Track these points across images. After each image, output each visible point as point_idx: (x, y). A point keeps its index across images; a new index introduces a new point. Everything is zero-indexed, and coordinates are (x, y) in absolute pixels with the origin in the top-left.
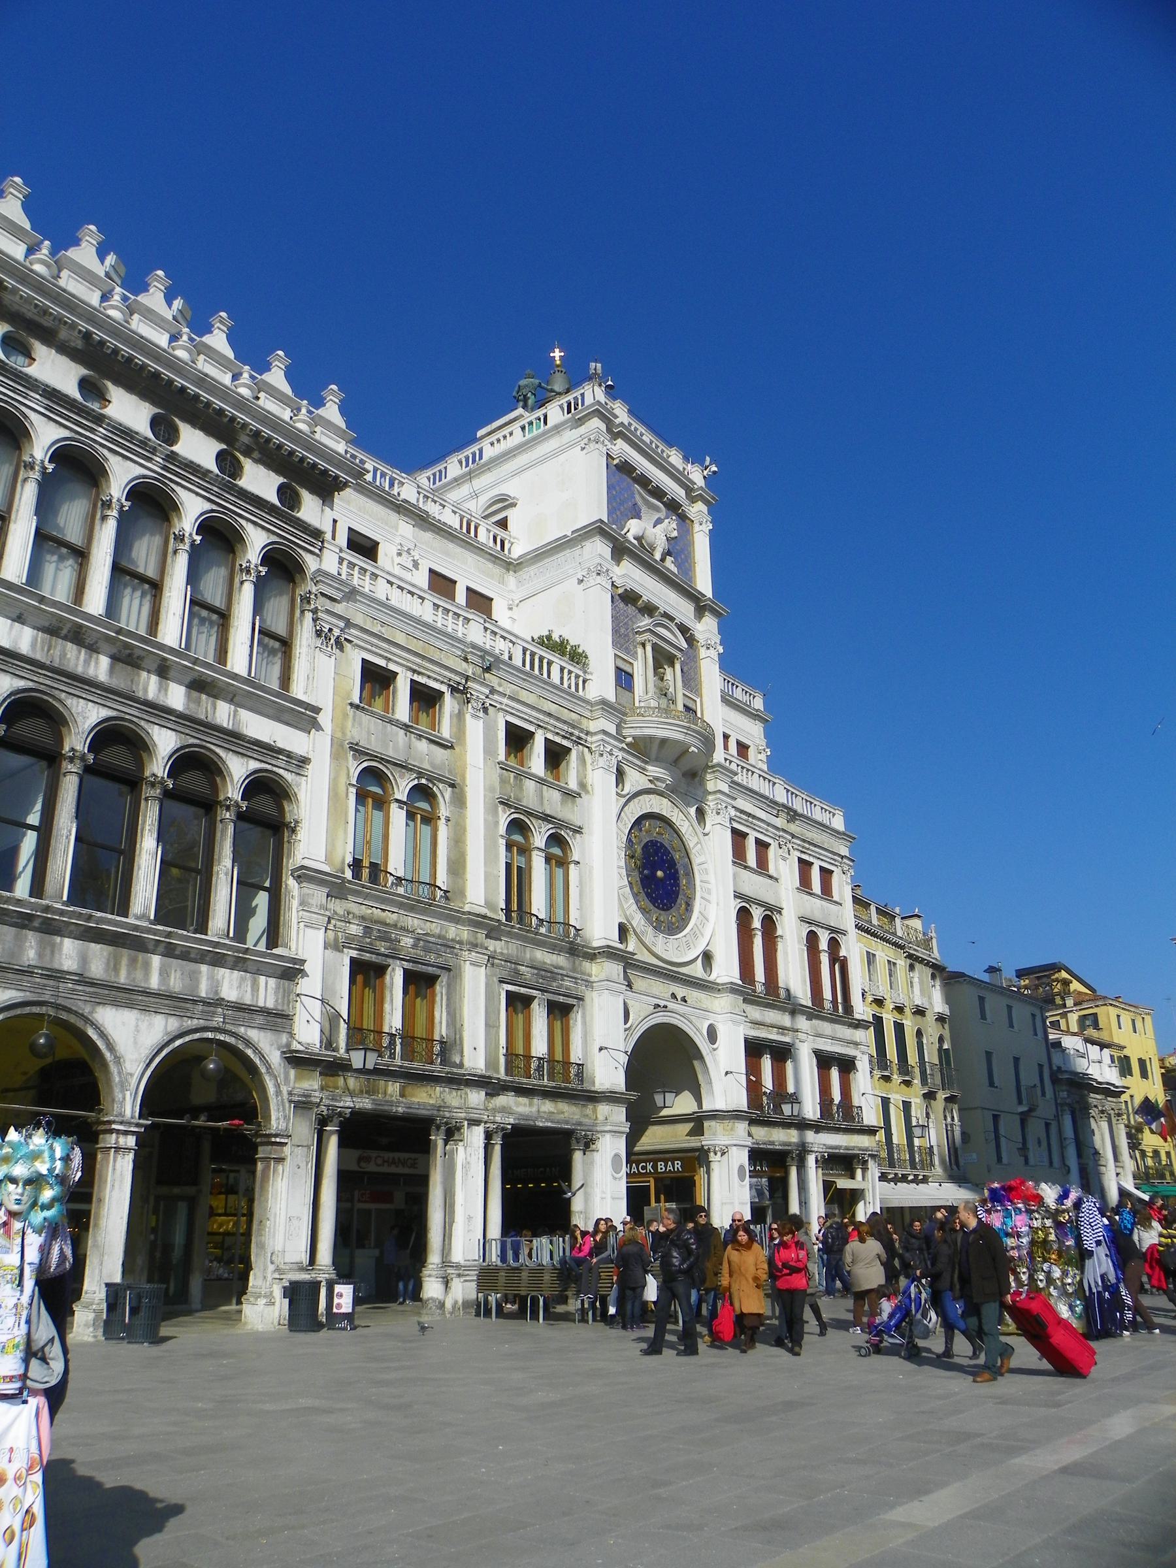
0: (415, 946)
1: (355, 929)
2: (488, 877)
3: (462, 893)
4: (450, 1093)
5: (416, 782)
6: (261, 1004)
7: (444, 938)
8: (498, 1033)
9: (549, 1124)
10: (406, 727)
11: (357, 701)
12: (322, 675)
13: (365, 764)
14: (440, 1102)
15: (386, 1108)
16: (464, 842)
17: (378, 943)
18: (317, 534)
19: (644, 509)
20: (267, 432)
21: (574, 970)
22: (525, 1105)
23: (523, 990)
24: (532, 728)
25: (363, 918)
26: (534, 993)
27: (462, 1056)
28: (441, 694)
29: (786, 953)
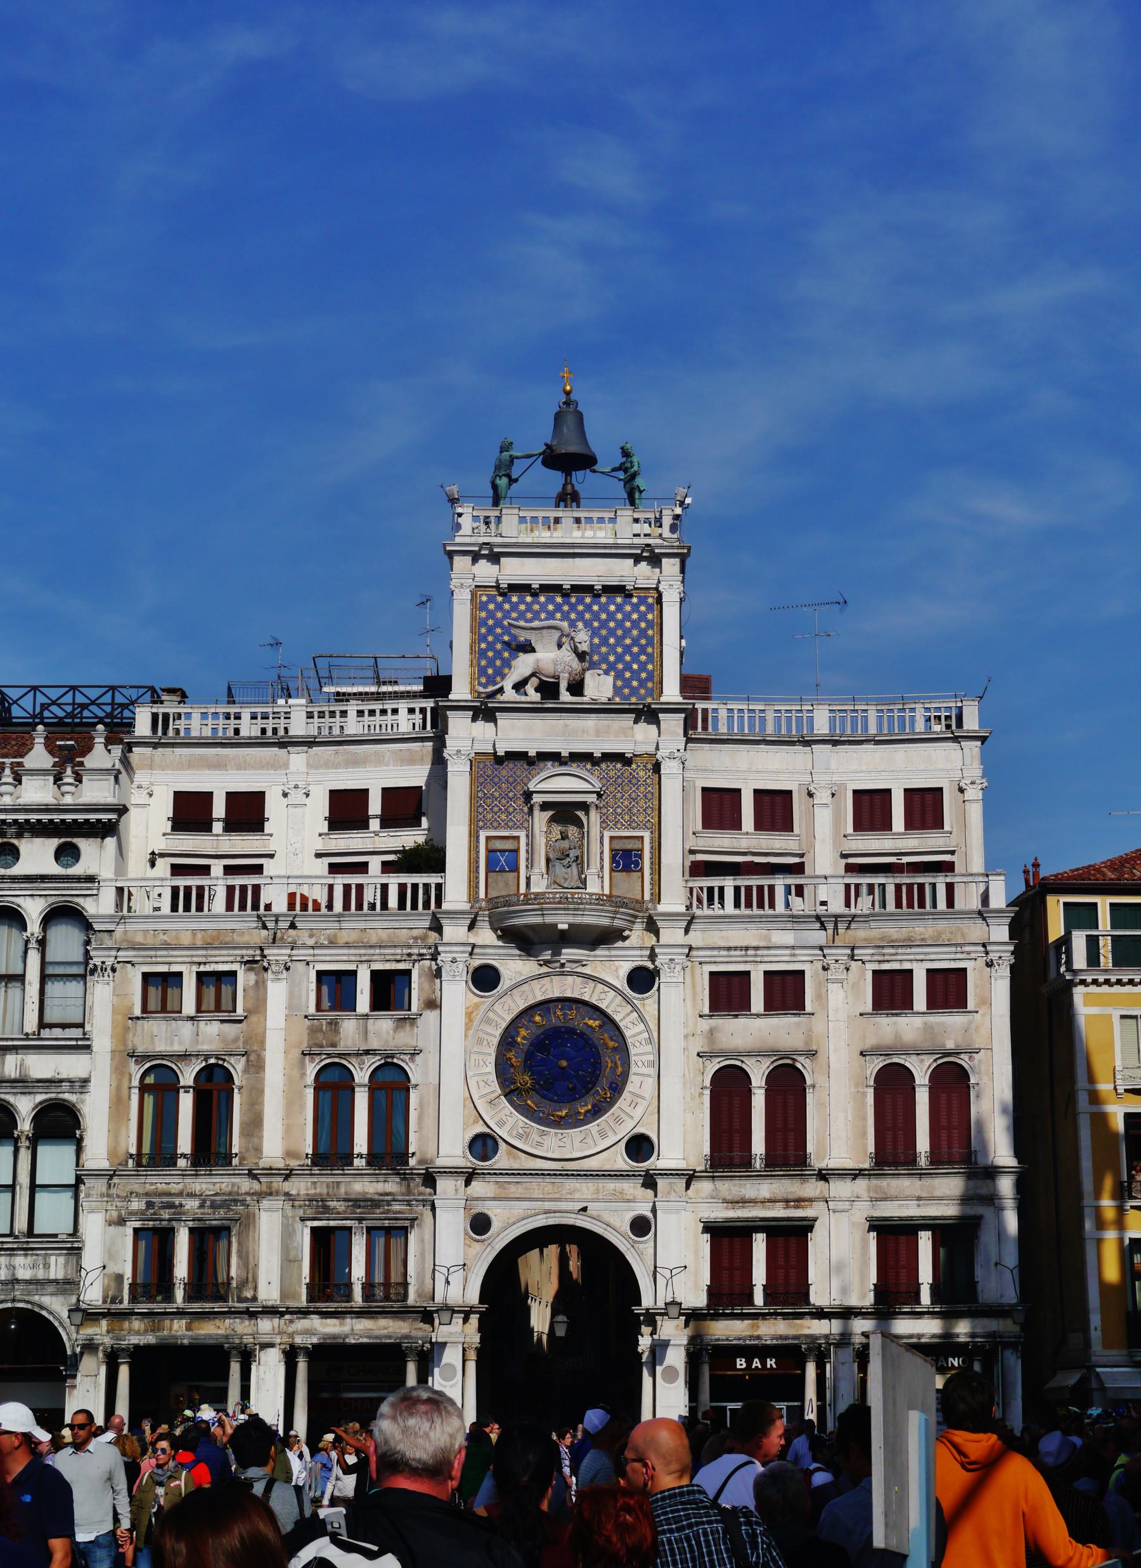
0: (202, 1206)
1: (137, 1205)
2: (288, 1129)
3: (258, 1150)
4: (241, 1323)
5: (204, 1064)
6: (52, 1277)
7: (238, 1194)
8: (300, 1268)
9: (365, 1340)
10: (192, 1018)
11: (137, 1012)
12: (106, 1002)
13: (148, 1065)
14: (229, 1332)
15: (171, 1341)
16: (262, 1104)
17: (162, 1212)
18: (91, 879)
19: (533, 637)
20: (21, 817)
21: (409, 1192)
22: (335, 1325)
23: (332, 1223)
24: (352, 967)
25: (147, 1194)
26: (348, 1223)
27: (255, 1289)
28: (233, 974)
29: (821, 1105)
